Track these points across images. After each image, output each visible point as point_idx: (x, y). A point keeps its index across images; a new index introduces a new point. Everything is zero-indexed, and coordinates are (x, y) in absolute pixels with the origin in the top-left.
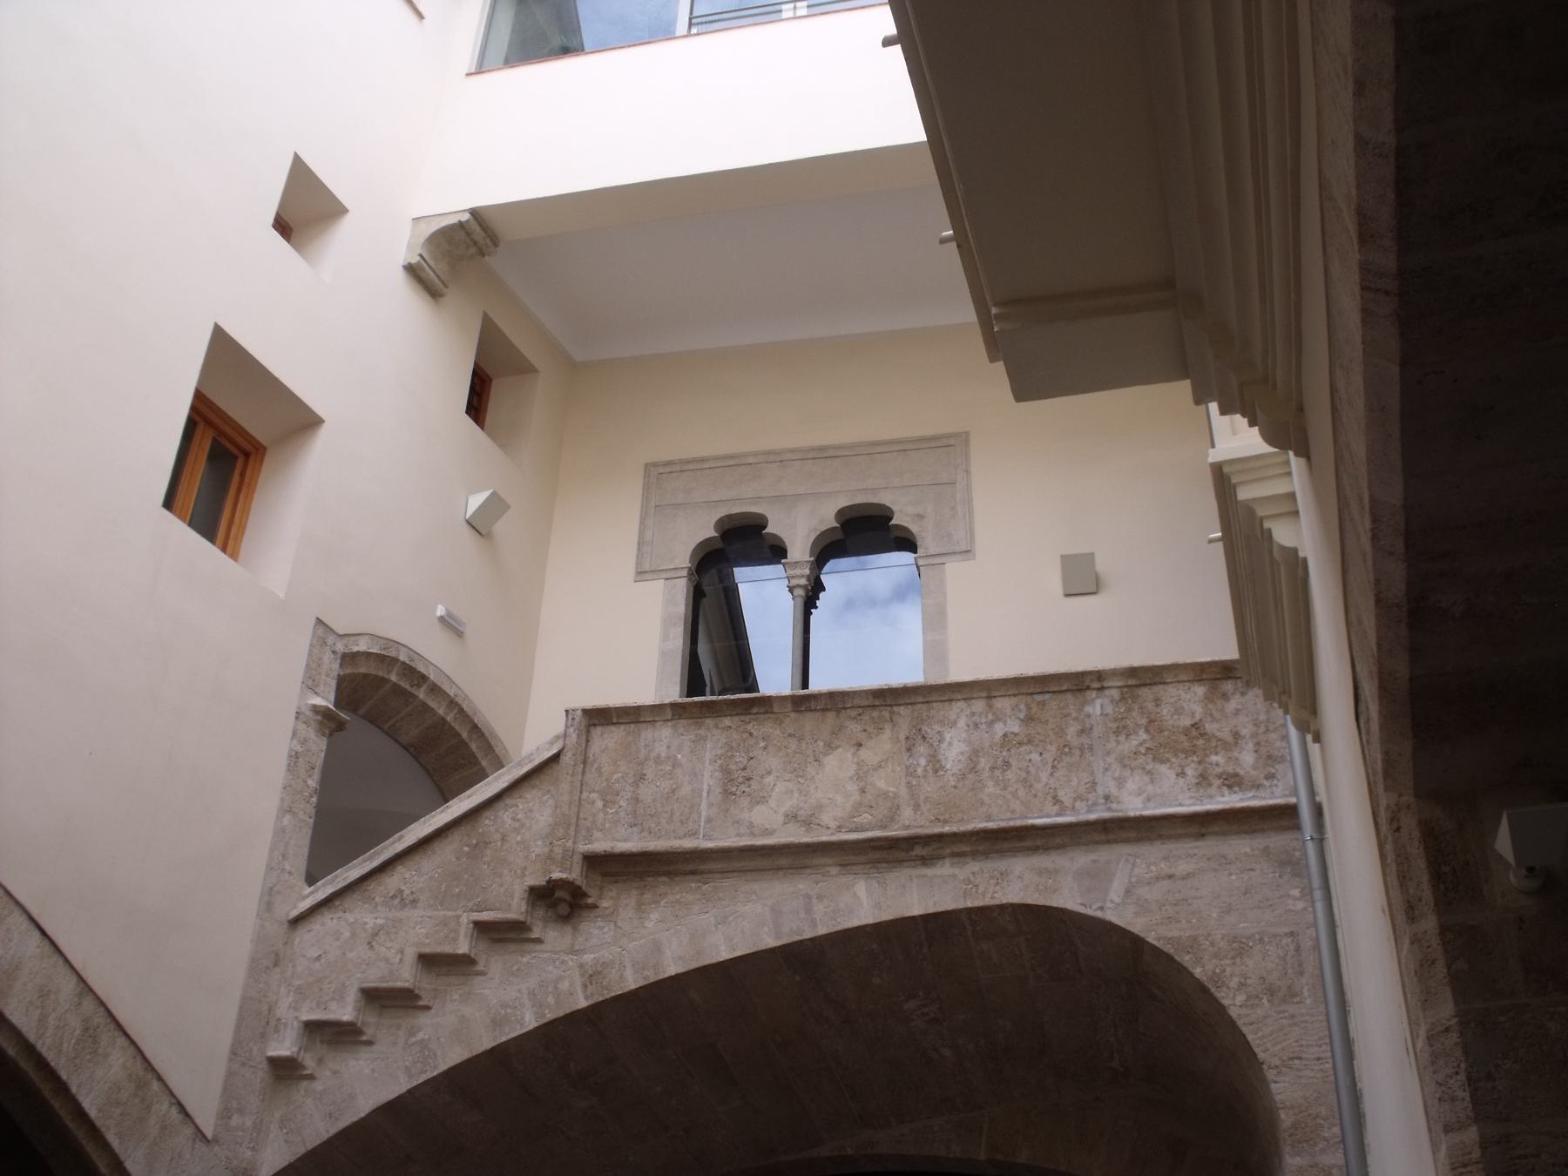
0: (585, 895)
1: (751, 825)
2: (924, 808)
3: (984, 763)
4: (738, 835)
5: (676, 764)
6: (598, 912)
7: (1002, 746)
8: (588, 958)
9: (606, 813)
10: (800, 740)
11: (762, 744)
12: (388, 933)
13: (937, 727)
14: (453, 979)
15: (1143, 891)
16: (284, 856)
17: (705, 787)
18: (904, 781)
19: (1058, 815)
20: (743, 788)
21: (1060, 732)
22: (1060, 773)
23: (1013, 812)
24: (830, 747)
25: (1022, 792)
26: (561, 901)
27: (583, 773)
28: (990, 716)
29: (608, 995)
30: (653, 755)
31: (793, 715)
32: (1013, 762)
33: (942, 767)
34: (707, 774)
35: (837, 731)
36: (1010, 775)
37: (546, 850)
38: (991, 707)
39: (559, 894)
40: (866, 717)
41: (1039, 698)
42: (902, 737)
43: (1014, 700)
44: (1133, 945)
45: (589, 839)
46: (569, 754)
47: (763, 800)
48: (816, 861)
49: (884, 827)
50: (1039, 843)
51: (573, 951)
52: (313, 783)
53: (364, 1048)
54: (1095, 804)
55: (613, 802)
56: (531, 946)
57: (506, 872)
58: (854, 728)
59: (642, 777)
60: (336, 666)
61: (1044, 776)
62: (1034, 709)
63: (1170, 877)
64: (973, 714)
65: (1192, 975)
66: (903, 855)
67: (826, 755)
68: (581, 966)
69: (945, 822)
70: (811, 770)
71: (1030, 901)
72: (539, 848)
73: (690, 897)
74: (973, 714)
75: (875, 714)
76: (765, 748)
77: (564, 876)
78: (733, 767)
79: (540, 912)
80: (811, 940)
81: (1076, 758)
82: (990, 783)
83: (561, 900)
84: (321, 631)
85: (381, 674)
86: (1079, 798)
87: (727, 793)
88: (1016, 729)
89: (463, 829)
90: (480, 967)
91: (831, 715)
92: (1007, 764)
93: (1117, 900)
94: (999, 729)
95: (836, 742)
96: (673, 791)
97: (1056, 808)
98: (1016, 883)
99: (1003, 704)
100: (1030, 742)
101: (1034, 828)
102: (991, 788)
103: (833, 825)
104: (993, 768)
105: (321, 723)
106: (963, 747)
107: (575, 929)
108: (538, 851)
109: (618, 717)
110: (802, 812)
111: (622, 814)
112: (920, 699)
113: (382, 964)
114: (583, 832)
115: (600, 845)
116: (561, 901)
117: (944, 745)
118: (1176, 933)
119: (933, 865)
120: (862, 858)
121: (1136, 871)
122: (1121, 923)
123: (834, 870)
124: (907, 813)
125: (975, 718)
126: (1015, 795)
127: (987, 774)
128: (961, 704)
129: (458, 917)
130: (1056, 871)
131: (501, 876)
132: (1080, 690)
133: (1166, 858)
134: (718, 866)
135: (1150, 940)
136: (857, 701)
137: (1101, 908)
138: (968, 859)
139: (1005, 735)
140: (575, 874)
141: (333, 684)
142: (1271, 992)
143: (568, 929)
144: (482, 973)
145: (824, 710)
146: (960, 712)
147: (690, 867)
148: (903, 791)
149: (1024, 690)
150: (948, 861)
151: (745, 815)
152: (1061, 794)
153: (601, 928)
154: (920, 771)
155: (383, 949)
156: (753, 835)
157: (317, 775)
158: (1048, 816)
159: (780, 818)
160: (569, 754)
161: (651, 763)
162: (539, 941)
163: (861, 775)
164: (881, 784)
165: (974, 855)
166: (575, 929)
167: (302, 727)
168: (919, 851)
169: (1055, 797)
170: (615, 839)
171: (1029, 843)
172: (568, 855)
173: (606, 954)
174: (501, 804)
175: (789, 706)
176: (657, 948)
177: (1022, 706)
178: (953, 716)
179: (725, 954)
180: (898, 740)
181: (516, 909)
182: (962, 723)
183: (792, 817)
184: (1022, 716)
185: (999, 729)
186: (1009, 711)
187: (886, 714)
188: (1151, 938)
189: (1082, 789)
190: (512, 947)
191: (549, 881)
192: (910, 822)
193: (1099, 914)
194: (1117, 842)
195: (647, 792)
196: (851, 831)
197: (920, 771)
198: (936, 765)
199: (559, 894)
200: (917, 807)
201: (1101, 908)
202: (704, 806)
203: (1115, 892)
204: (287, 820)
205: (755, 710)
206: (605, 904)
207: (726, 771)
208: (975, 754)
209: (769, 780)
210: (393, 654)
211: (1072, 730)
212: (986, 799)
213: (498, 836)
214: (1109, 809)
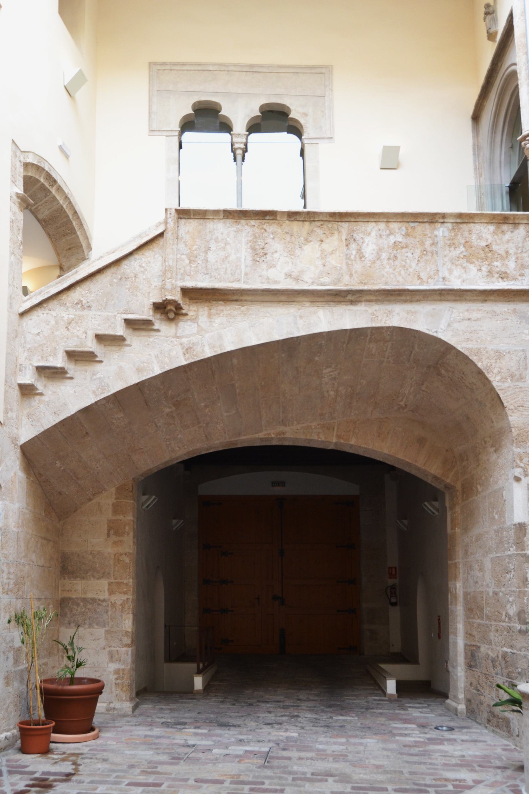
0: (181, 308)
1: (268, 278)
2: (355, 276)
3: (384, 256)
4: (262, 283)
5: (226, 243)
6: (187, 317)
7: (394, 248)
8: (184, 340)
9: (191, 267)
10: (292, 236)
11: (272, 236)
12: (77, 323)
13: (361, 235)
14: (114, 348)
15: (456, 325)
17: (243, 257)
18: (344, 262)
19: (419, 285)
20: (263, 258)
21: (422, 243)
22: (422, 264)
23: (398, 281)
24: (307, 241)
25: (403, 272)
26: (168, 310)
27: (177, 244)
28: (388, 232)
29: (197, 359)
30: (214, 237)
31: (287, 222)
32: (399, 256)
33: (364, 256)
35: (311, 233)
36: (397, 263)
37: (160, 284)
38: (388, 227)
39: (169, 307)
40: (325, 226)
41: (412, 225)
42: (344, 238)
43: (399, 225)
44: (448, 348)
45: (183, 279)
46: (170, 233)
47: (273, 266)
49: (335, 284)
50: (408, 298)
51: (176, 336)
53: (68, 381)
54: (438, 281)
55: (194, 261)
56: (154, 333)
57: (139, 294)
58: (319, 231)
59: (209, 249)
61: (414, 265)
62: (410, 230)
63: (469, 319)
64: (379, 230)
65: (476, 366)
67: (305, 244)
68: (181, 344)
69: (365, 284)
70: (298, 252)
72: (156, 283)
73: (236, 313)
74: (379, 230)
75: (330, 225)
76: (273, 238)
77: (173, 298)
78: (257, 247)
79: (158, 316)
80: (297, 337)
81: (429, 257)
82: (388, 267)
83: (171, 310)
86: (430, 277)
87: (255, 261)
88: (400, 240)
89: (113, 270)
90: (127, 342)
91: (307, 224)
92: (396, 257)
93: (444, 328)
94: (392, 239)
95: (310, 239)
96: (226, 257)
97: (419, 281)
99: (394, 226)
100: (407, 247)
101: (408, 290)
102: (388, 269)
103: (310, 281)
104: (389, 259)
106: (374, 247)
107: (177, 325)
108: (155, 284)
110: (293, 274)
111: (200, 268)
112: (353, 220)
113: (75, 339)
114: (179, 276)
115: (190, 284)
116: (168, 310)
117: (365, 245)
118: (470, 346)
121: (453, 315)
122: (446, 340)
124: (346, 278)
125: (380, 232)
126: (399, 274)
127: (385, 262)
128: (373, 224)
129: (115, 316)
130: (416, 312)
131: (136, 296)
133: (467, 310)
136: (321, 218)
137: (436, 332)
139: (395, 243)
140: (177, 297)
142: (512, 376)
143: (173, 325)
144: (129, 345)
145: (303, 221)
146: (373, 229)
148: (344, 267)
149: (405, 220)
151: (264, 273)
152: (422, 275)
153: (190, 326)
154: (352, 257)
155: (75, 331)
158: (415, 285)
159: (283, 275)
160: (170, 233)
161: (213, 241)
162: (158, 330)
163: (324, 255)
164: (333, 262)
165: (377, 301)
166: (177, 325)
169: (418, 276)
170: (197, 281)
172: (174, 288)
173: (194, 339)
174: (132, 258)
175: (285, 218)
176: (220, 337)
177: (404, 228)
178: (369, 230)
179: (254, 342)
180: (342, 241)
181: (145, 313)
182: (373, 234)
183: (289, 275)
184: (403, 233)
185: (392, 239)
186: (397, 230)
187: (335, 225)
188: (459, 348)
189: (432, 273)
190: (143, 333)
191: (164, 301)
193: (435, 335)
194: (445, 300)
195: (212, 257)
197: (352, 257)
198: (361, 256)
199: (169, 307)
200: (351, 275)
201: (436, 332)
202: (243, 267)
203: (443, 325)
205: (268, 218)
206: (191, 313)
207: (253, 249)
208: (380, 250)
209: (276, 255)
212: (386, 275)
213: (133, 275)
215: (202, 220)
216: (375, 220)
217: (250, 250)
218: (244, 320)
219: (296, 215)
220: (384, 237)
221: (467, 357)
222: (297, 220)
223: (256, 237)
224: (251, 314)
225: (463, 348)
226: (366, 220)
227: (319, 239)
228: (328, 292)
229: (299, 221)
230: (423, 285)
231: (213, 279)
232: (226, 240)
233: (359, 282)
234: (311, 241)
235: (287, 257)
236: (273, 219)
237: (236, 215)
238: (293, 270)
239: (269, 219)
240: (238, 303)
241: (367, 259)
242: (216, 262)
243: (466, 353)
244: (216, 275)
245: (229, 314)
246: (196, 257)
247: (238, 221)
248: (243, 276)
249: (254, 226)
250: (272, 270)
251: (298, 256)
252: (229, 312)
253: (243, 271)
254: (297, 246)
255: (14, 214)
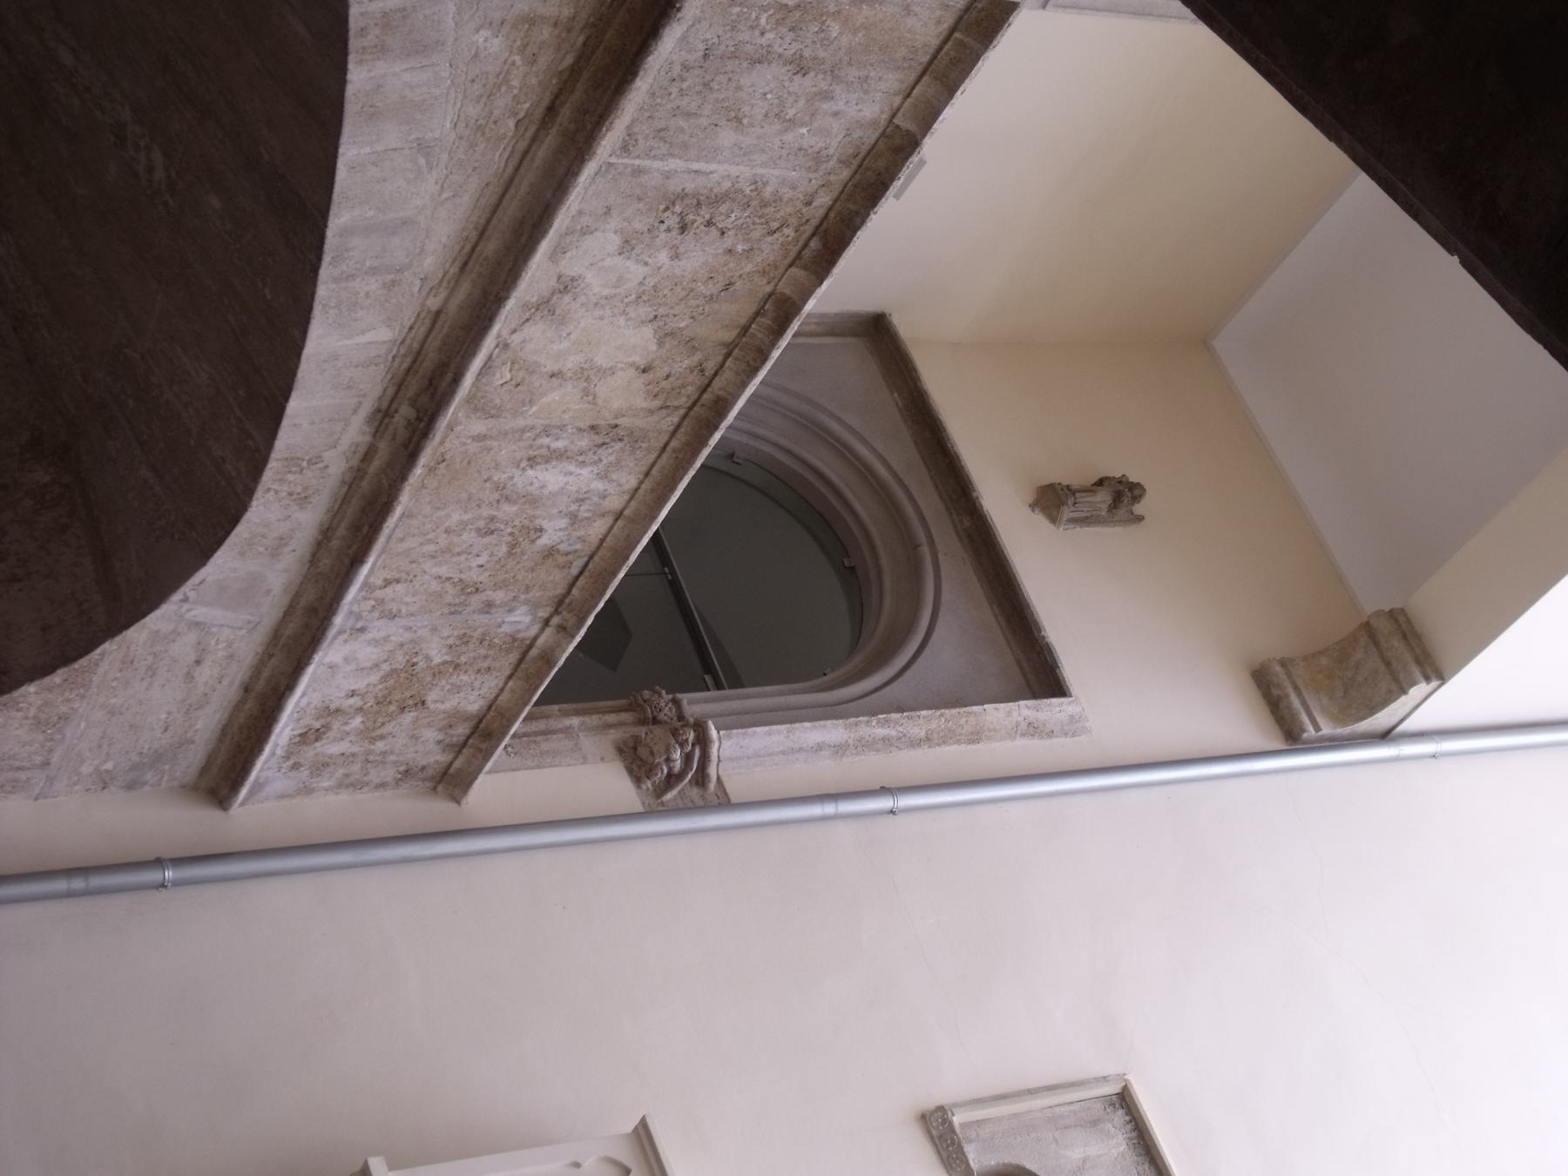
1: (586, 231)
34: (734, 170)
48: (465, 288)
50: (335, 543)
59: (802, 71)
66: (410, 392)
69: (431, 470)
71: (239, 529)
73: (502, 101)
96: (739, 120)
98: (280, 518)
109: (961, 43)
111: (745, 36)
119: (370, 419)
120: (435, 342)
123: (434, 303)
132: (560, 602)
134: (541, 154)
135: (106, 645)
136: (726, 377)
138: (355, 462)
145: (745, 330)
147: (565, 112)
150: (368, 438)
151: (615, 222)
152: (399, 587)
156: (569, 232)
165: (357, 474)
168: (405, 411)
171: (342, 531)
175: (784, 288)
192: (458, 425)
196: (490, 358)
205: (815, 244)
209: (663, 257)
211: (499, 596)
214: (340, 632)
215: (925, 59)
216: (641, 492)
217: (727, 185)
218: (461, 125)
219: (774, 320)
220: (574, 507)
221: (67, 660)
222: (757, 314)
223: (764, 205)
224: (472, 145)
225: (102, 655)
226: (654, 471)
227: (657, 363)
228: (450, 375)
229: (753, 319)
230: (361, 589)
231: (677, 70)
232: (803, 124)
233: (448, 456)
234: (660, 344)
235: (641, 284)
236: (799, 255)
237: (881, 164)
238: (582, 299)
239: (806, 245)
240: (540, 111)
241: (517, 473)
242: (739, 88)
243: (83, 662)
244: (685, 85)
245: (506, 81)
246: (792, 29)
247: (855, 163)
248: (637, 162)
249: (808, 203)
250: (615, 241)
251: (624, 313)
252: (515, 83)
253: (657, 164)
254: (662, 311)
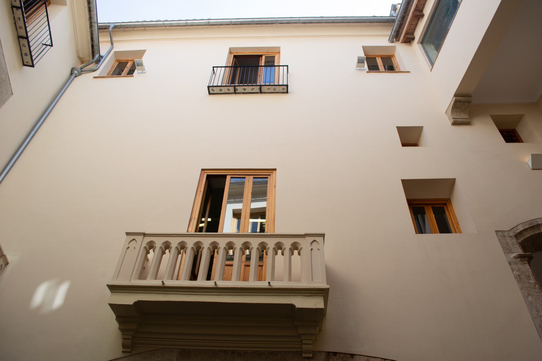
16: (537, 311)
52: (532, 281)
60: (514, 240)
84: (500, 234)
85: (537, 232)
105: (521, 261)
141: (517, 246)
157: (532, 278)
167: (514, 266)
204: (530, 298)
210: (536, 224)
255: (519, 270)
